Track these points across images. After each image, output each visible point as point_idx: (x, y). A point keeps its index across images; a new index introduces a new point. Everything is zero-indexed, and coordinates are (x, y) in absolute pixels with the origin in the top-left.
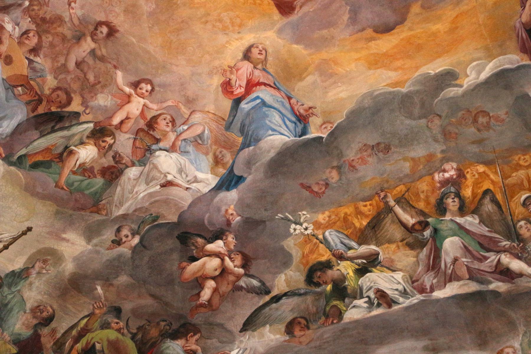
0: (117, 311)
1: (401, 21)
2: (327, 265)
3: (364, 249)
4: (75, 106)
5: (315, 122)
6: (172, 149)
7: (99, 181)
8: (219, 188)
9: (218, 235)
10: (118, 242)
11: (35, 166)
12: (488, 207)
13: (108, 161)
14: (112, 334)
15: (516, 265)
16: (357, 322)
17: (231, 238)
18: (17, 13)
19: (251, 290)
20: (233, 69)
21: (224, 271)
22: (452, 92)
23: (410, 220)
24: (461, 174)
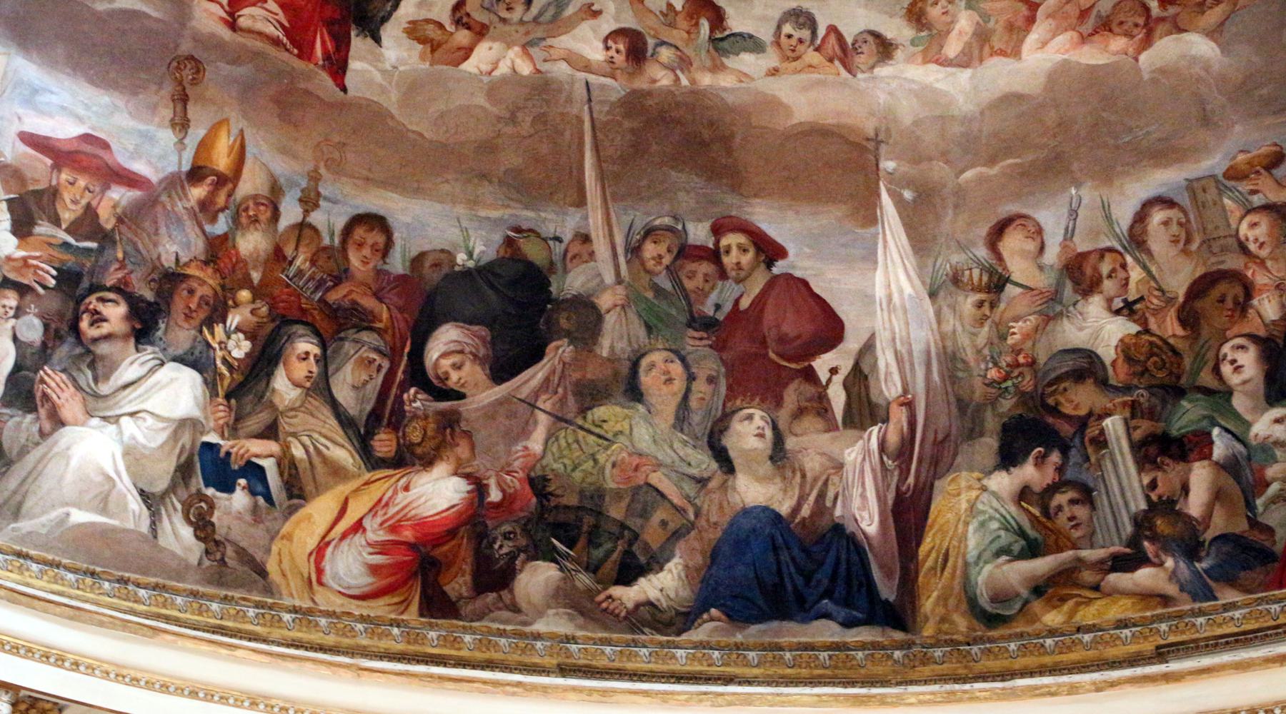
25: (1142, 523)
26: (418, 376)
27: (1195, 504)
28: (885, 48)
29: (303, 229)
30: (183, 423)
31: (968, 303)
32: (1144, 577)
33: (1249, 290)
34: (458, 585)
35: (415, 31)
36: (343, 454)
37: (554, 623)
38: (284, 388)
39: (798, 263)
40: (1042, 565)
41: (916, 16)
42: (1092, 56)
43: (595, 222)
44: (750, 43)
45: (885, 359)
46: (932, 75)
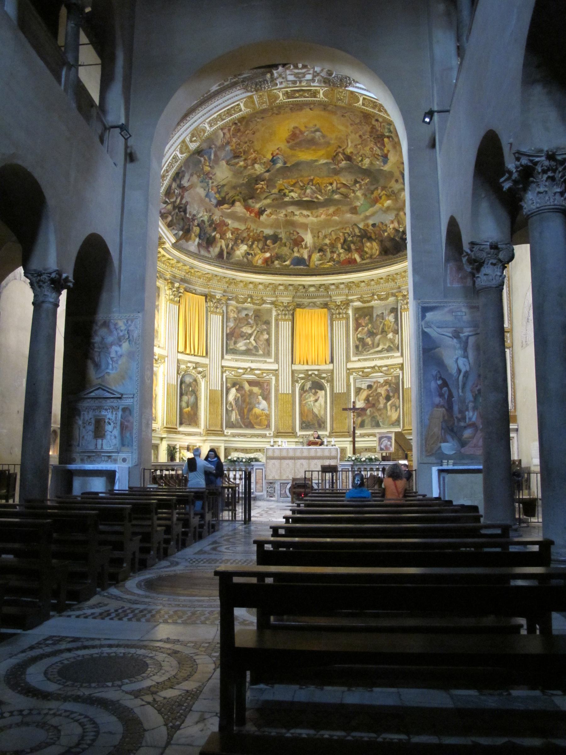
0: (241, 193)
2: (283, 190)
3: (291, 188)
4: (242, 155)
7: (243, 168)
9: (263, 181)
10: (243, 180)
12: (317, 185)
13: (245, 165)
15: (320, 197)
17: (265, 182)
19: (267, 192)
20: (275, 151)
21: (263, 188)
23: (302, 184)
24: (314, 179)
26: (266, 245)
28: (308, 216)
29: (256, 232)
30: (246, 250)
31: (316, 238)
32: (330, 263)
35: (267, 215)
36: (259, 252)
38: (254, 246)
40: (321, 262)
41: (312, 213)
44: (296, 215)
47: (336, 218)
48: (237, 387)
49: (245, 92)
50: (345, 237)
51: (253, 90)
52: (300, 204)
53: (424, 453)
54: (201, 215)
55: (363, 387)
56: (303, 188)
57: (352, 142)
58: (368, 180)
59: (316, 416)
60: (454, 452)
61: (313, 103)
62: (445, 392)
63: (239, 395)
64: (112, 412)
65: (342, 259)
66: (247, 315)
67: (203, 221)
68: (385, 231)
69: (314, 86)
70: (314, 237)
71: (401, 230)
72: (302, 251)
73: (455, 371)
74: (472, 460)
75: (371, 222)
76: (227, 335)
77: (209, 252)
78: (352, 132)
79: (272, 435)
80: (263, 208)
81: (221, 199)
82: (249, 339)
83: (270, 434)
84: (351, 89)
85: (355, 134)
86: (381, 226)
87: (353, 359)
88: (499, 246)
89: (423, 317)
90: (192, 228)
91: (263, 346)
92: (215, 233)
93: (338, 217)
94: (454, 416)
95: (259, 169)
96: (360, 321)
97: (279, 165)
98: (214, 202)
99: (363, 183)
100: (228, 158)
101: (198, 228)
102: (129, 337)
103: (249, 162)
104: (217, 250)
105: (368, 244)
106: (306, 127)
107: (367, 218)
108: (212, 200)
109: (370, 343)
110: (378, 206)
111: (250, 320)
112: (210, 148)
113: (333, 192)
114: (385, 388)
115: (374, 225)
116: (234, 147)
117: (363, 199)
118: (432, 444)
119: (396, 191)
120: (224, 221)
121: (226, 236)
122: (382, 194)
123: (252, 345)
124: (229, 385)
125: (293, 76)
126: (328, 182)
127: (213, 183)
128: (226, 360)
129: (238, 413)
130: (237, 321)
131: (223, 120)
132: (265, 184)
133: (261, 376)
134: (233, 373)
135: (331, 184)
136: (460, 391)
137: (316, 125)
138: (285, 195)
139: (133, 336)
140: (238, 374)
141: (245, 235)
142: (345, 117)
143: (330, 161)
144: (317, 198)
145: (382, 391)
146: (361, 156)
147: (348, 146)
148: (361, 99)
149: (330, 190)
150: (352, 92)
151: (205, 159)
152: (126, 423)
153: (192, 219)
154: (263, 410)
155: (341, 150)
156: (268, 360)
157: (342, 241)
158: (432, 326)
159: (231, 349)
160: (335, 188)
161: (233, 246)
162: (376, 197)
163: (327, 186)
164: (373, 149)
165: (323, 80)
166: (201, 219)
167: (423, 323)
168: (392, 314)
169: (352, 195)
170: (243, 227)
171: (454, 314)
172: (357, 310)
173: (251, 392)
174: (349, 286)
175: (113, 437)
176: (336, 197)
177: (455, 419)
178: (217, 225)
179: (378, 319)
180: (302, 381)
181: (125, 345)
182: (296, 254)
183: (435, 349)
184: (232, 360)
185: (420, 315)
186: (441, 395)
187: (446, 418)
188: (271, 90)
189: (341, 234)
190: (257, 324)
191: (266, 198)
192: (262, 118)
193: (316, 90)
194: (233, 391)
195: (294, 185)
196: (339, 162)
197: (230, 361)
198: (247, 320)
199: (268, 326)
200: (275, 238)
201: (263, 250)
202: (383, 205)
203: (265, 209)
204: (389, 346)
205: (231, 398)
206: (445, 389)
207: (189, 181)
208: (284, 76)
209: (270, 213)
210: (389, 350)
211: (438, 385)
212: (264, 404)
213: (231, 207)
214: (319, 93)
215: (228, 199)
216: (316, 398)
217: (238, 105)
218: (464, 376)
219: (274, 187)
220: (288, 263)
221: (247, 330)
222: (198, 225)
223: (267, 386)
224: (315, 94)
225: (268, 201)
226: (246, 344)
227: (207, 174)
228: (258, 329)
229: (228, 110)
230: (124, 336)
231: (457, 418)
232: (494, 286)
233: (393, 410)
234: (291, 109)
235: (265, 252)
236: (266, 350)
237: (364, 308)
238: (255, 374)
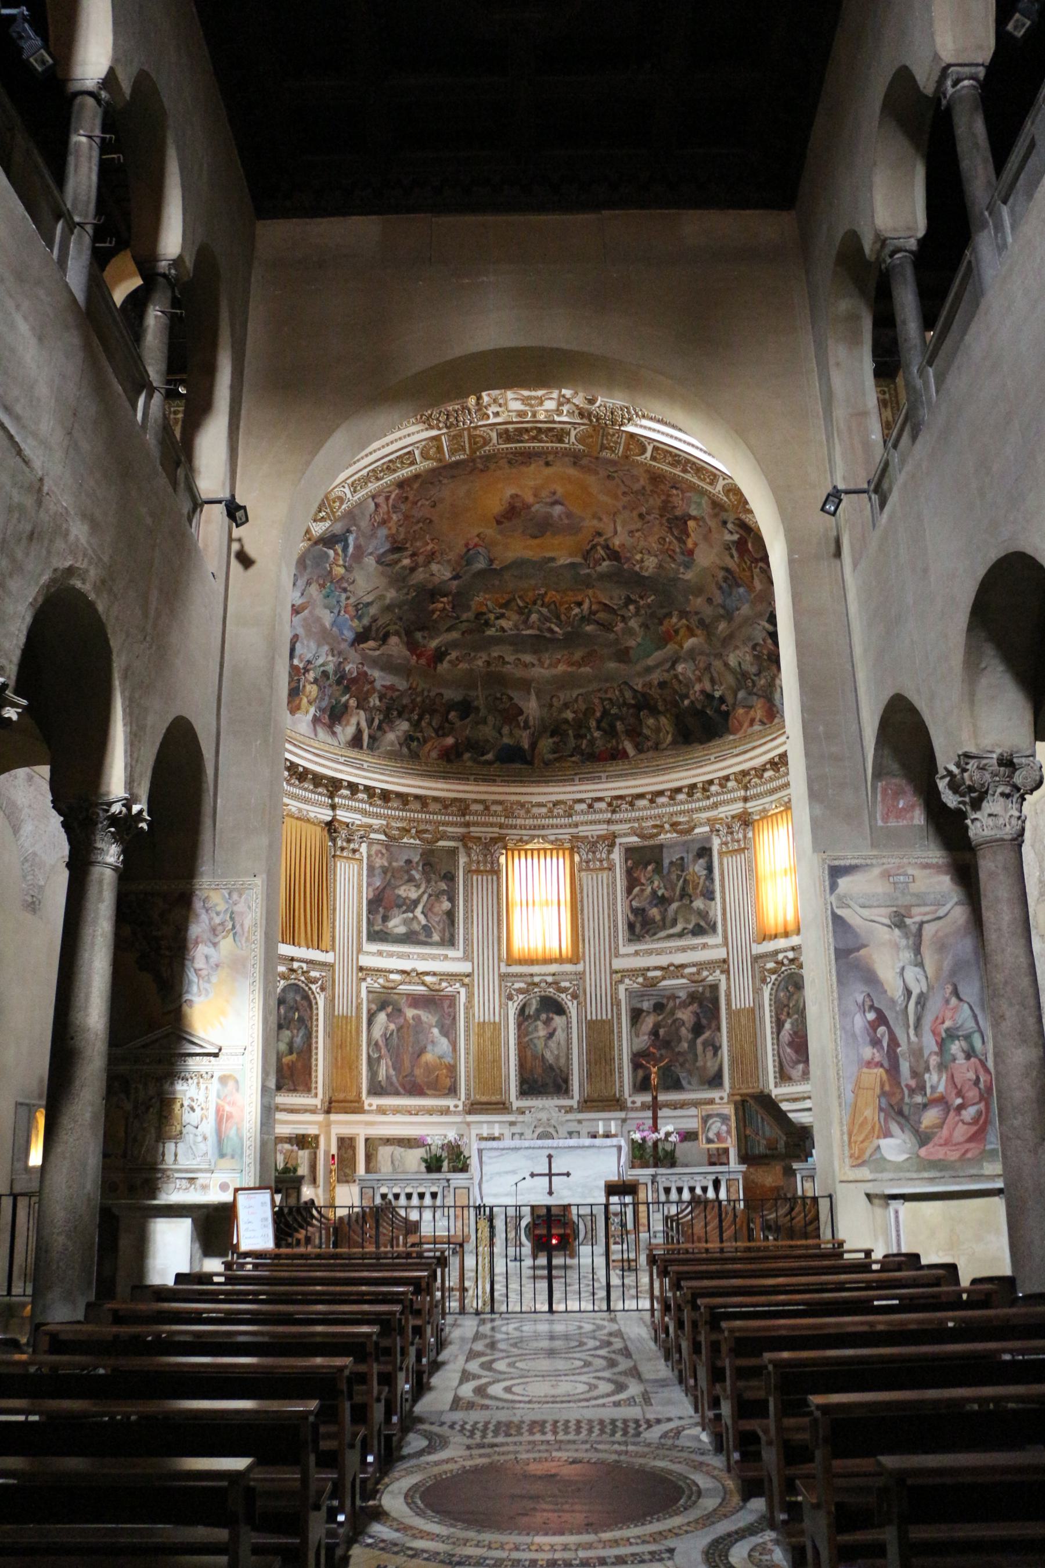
0: (401, 619)
1: (542, 536)
2: (484, 614)
4: (408, 545)
5: (497, 562)
6: (438, 563)
8: (451, 579)
9: (445, 596)
10: (407, 594)
11: (387, 565)
12: (553, 606)
13: (413, 565)
14: (397, 627)
15: (557, 629)
16: (490, 636)
17: (450, 598)
18: (399, 514)
21: (444, 609)
22: (554, 565)
23: (521, 604)
24: (546, 593)
25: (574, 749)
26: (447, 720)
27: (584, 747)
29: (428, 696)
30: (405, 732)
31: (546, 710)
32: (573, 759)
33: (595, 711)
34: (452, 757)
35: (450, 662)
36: (433, 735)
37: (469, 764)
38: (423, 724)
39: (516, 701)
40: (556, 755)
41: (539, 660)
42: (569, 669)
43: (480, 694)
45: (531, 718)
46: (542, 670)
47: (588, 669)
48: (389, 1009)
49: (427, 429)
50: (604, 707)
51: (441, 425)
52: (518, 643)
53: (847, 1160)
54: (320, 661)
55: (645, 1008)
56: (524, 612)
57: (623, 527)
58: (653, 597)
59: (551, 1067)
60: (906, 1156)
61: (556, 452)
62: (883, 1035)
63: (392, 1026)
64: (198, 1083)
65: (597, 751)
66: (409, 862)
67: (325, 674)
68: (687, 696)
69: (560, 422)
70: (541, 706)
71: (717, 694)
72: (517, 732)
73: (900, 992)
74: (941, 1170)
75: (656, 677)
76: (370, 903)
77: (334, 733)
78: (624, 507)
79: (460, 1108)
80: (443, 649)
81: (362, 630)
82: (412, 912)
83: (456, 1106)
84: (630, 428)
85: (631, 511)
86: (676, 687)
87: (623, 950)
88: (1015, 760)
89: (833, 886)
90: (304, 686)
91: (441, 925)
92: (347, 696)
93: (591, 667)
94: (903, 1084)
95: (441, 572)
96: (635, 875)
97: (481, 564)
98: (349, 635)
99: (642, 603)
100: (382, 551)
101: (315, 687)
102: (234, 927)
103: (421, 559)
104: (351, 730)
105: (651, 721)
106: (535, 496)
107: (649, 670)
108: (345, 632)
109: (658, 918)
110: (671, 647)
111: (413, 872)
112: (349, 531)
113: (583, 618)
114: (690, 1008)
115: (662, 685)
116: (394, 531)
117: (642, 633)
118: (862, 1142)
119: (707, 621)
120: (366, 673)
121: (369, 702)
122: (680, 624)
123: (419, 923)
124: (374, 1007)
125: (519, 403)
126: (573, 599)
127: (348, 598)
128: (368, 953)
129: (390, 1063)
130: (389, 875)
131: (378, 479)
132: (448, 603)
133: (437, 987)
134: (381, 981)
135: (579, 604)
136: (912, 1032)
137: (554, 493)
138: (487, 624)
139: (242, 925)
140: (391, 985)
141: (405, 701)
142: (613, 478)
143: (578, 560)
144: (551, 631)
145: (686, 1015)
146: (641, 553)
147: (616, 533)
148: (650, 449)
149: (576, 615)
150: (632, 436)
151: (336, 554)
152: (227, 1108)
153: (304, 668)
154: (440, 1058)
155: (601, 540)
156: (451, 953)
157: (598, 714)
158: (851, 903)
159: (377, 932)
160: (586, 612)
161: (381, 722)
162: (668, 632)
163: (570, 609)
164: (664, 539)
165: (577, 412)
166: (322, 669)
167: (833, 899)
168: (701, 861)
169: (621, 625)
170: (402, 684)
171: (891, 879)
172: (630, 852)
173: (417, 1019)
174: (615, 803)
175: (200, 1139)
176: (589, 628)
177: (905, 1089)
178: (354, 681)
179: (673, 869)
180: (521, 997)
181: (226, 944)
182: (506, 740)
183: (858, 949)
184: (380, 953)
185: (827, 883)
186: (876, 1043)
187: (887, 1088)
188: (475, 428)
189: (596, 701)
190: (428, 881)
191: (449, 630)
192: (453, 477)
193: (562, 429)
194: (382, 1017)
195: (505, 605)
196: (598, 562)
197: (375, 957)
198: (408, 872)
199: (451, 884)
200: (465, 708)
201: (441, 731)
202: (682, 647)
203: (447, 650)
204: (698, 925)
205: (377, 1033)
206: (882, 1029)
207: (302, 594)
208: (501, 401)
209: (457, 658)
210: (698, 931)
211: (869, 1022)
212: (444, 1044)
213: (380, 646)
214: (568, 434)
215: (378, 630)
216: (551, 1031)
217: (409, 453)
218: (917, 1003)
219: (468, 608)
220: (489, 756)
221: (410, 892)
222: (316, 681)
223: (450, 1006)
224: (560, 435)
225: (455, 635)
226: (405, 922)
227: (338, 582)
228: (430, 891)
229: (390, 461)
230: (222, 924)
231: (907, 1086)
232: (1010, 837)
233: (710, 1053)
234: (509, 462)
235: (444, 735)
236: (447, 934)
237: (645, 847)
238: (424, 984)
